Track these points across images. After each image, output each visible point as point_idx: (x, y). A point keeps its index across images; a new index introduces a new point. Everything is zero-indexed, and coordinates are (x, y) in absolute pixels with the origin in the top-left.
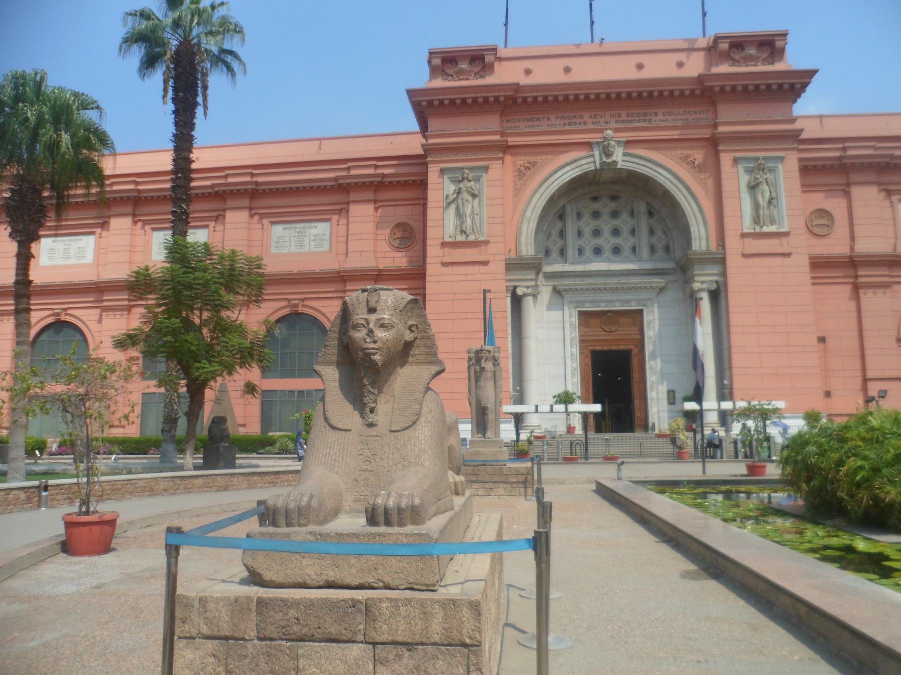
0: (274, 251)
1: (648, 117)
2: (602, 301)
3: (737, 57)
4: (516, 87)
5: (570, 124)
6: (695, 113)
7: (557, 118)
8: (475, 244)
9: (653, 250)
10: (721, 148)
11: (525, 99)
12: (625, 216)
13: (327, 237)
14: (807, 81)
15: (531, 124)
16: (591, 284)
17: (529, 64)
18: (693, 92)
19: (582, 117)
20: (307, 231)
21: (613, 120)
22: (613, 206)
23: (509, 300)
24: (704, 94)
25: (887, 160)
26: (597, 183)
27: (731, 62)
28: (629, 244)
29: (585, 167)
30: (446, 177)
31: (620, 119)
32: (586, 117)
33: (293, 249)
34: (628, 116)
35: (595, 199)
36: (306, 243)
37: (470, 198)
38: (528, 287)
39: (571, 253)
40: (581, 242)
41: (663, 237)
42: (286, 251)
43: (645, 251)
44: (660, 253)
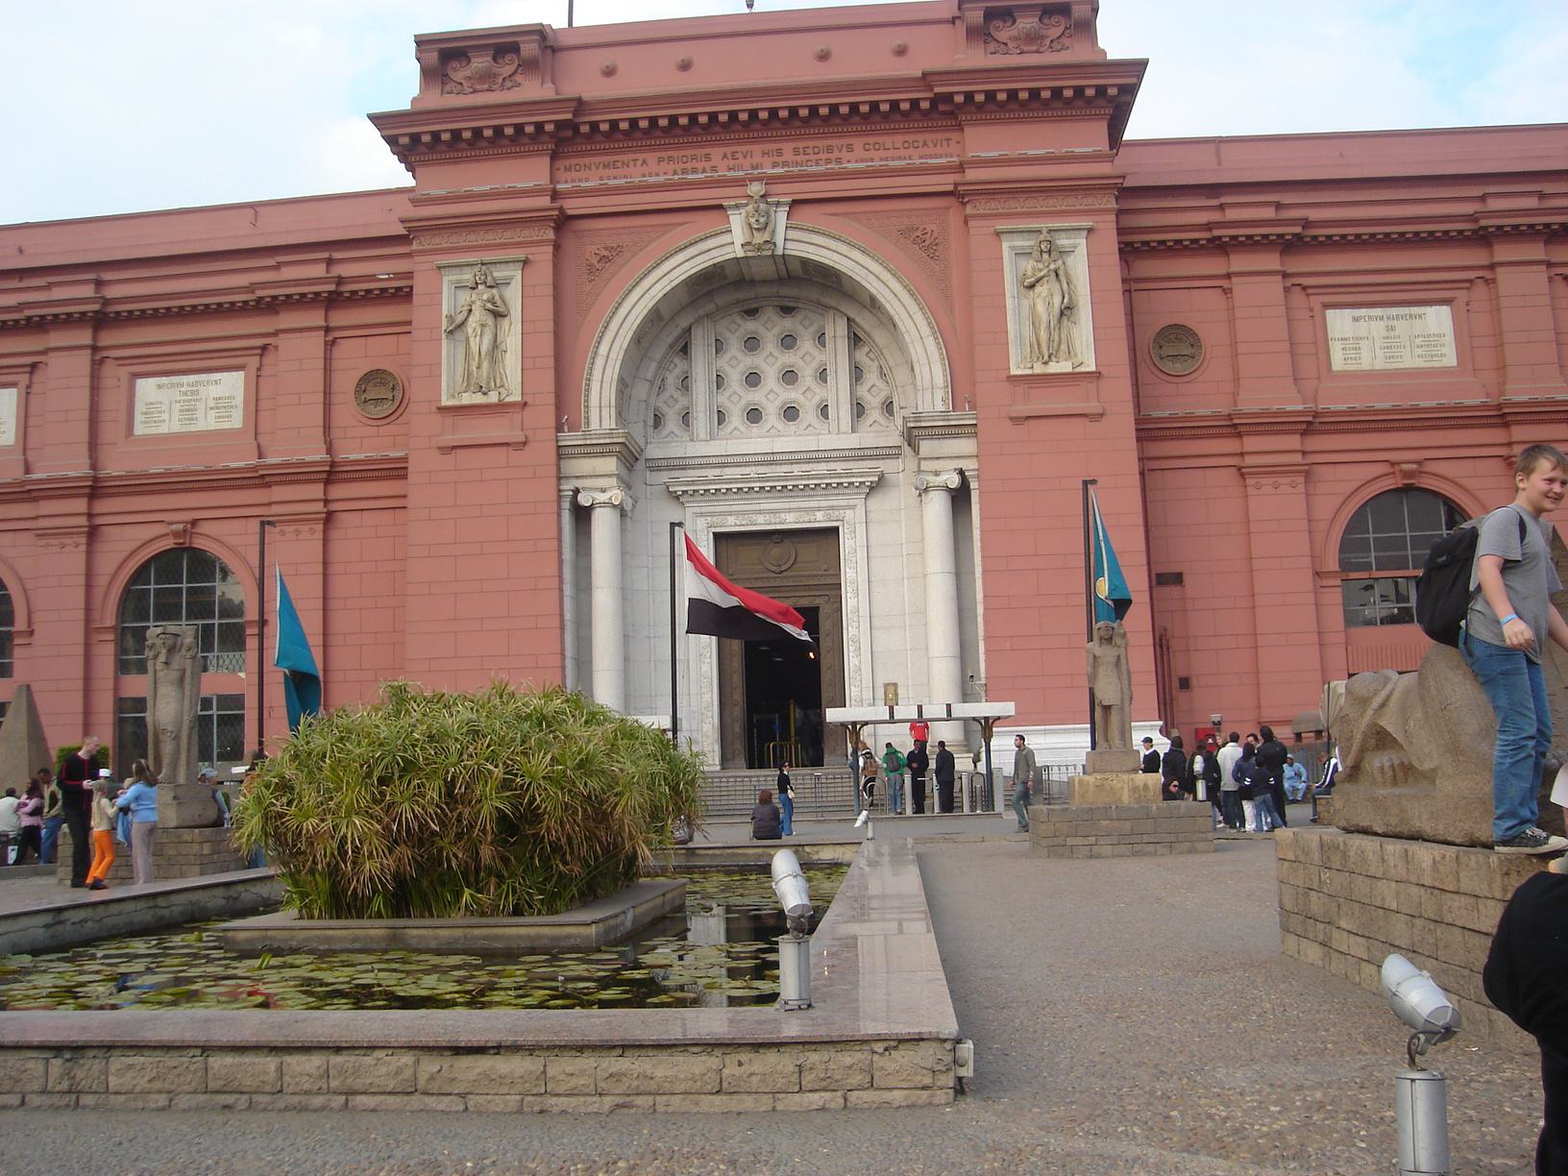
0: (139, 429)
1: (833, 156)
2: (760, 512)
3: (1003, 35)
4: (580, 105)
5: (684, 171)
6: (925, 144)
7: (660, 160)
8: (501, 407)
9: (859, 410)
10: (969, 210)
11: (595, 126)
12: (807, 344)
13: (239, 400)
14: (1134, 80)
15: (611, 172)
16: (736, 480)
17: (606, 58)
18: (915, 103)
19: (708, 158)
20: (201, 389)
21: (768, 161)
22: (787, 324)
23: (567, 517)
24: (939, 107)
25: (1298, 230)
26: (752, 282)
27: (992, 46)
28: (817, 399)
29: (714, 253)
30: (446, 279)
31: (780, 160)
32: (716, 153)
33: (176, 427)
34: (796, 151)
35: (752, 313)
36: (200, 414)
37: (490, 321)
38: (603, 491)
39: (701, 421)
40: (722, 399)
41: (880, 384)
42: (164, 429)
43: (843, 413)
44: (874, 414)
